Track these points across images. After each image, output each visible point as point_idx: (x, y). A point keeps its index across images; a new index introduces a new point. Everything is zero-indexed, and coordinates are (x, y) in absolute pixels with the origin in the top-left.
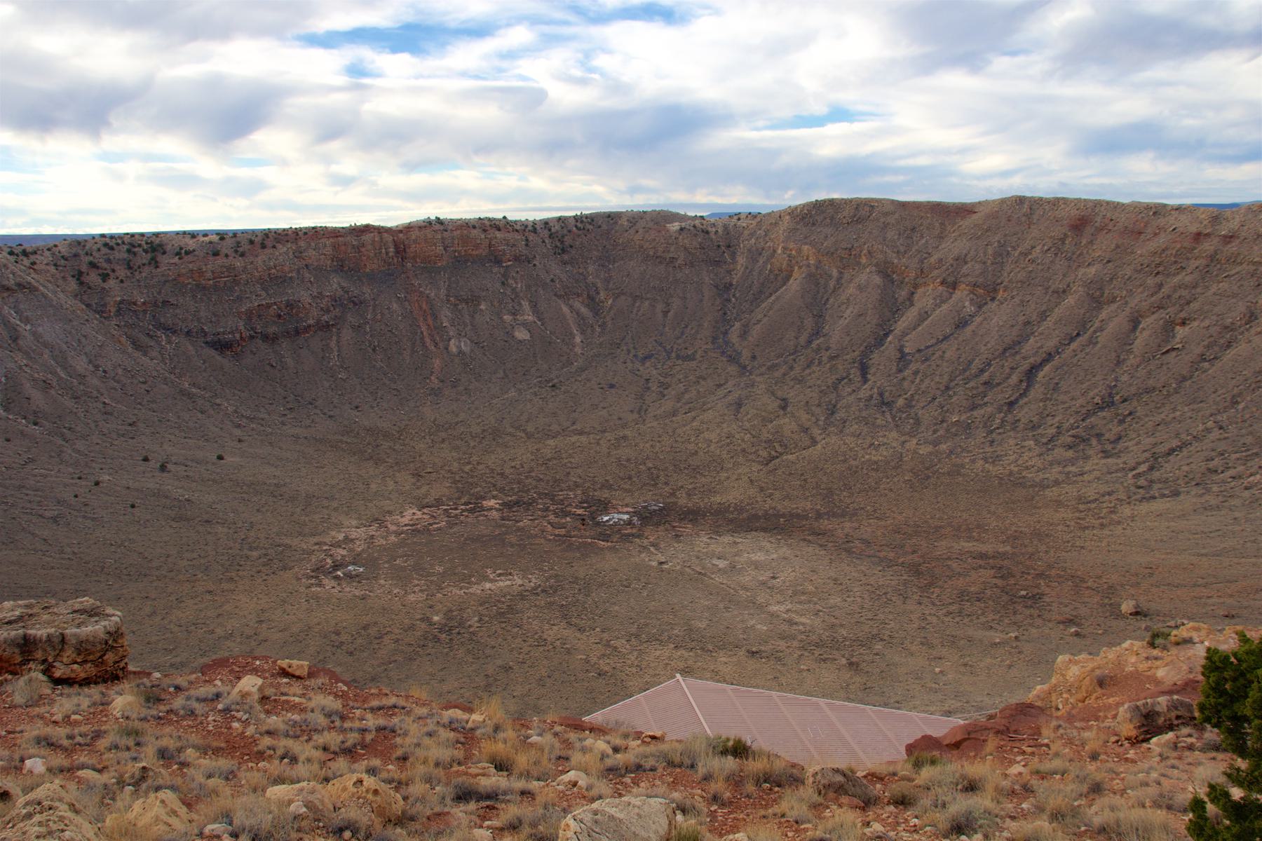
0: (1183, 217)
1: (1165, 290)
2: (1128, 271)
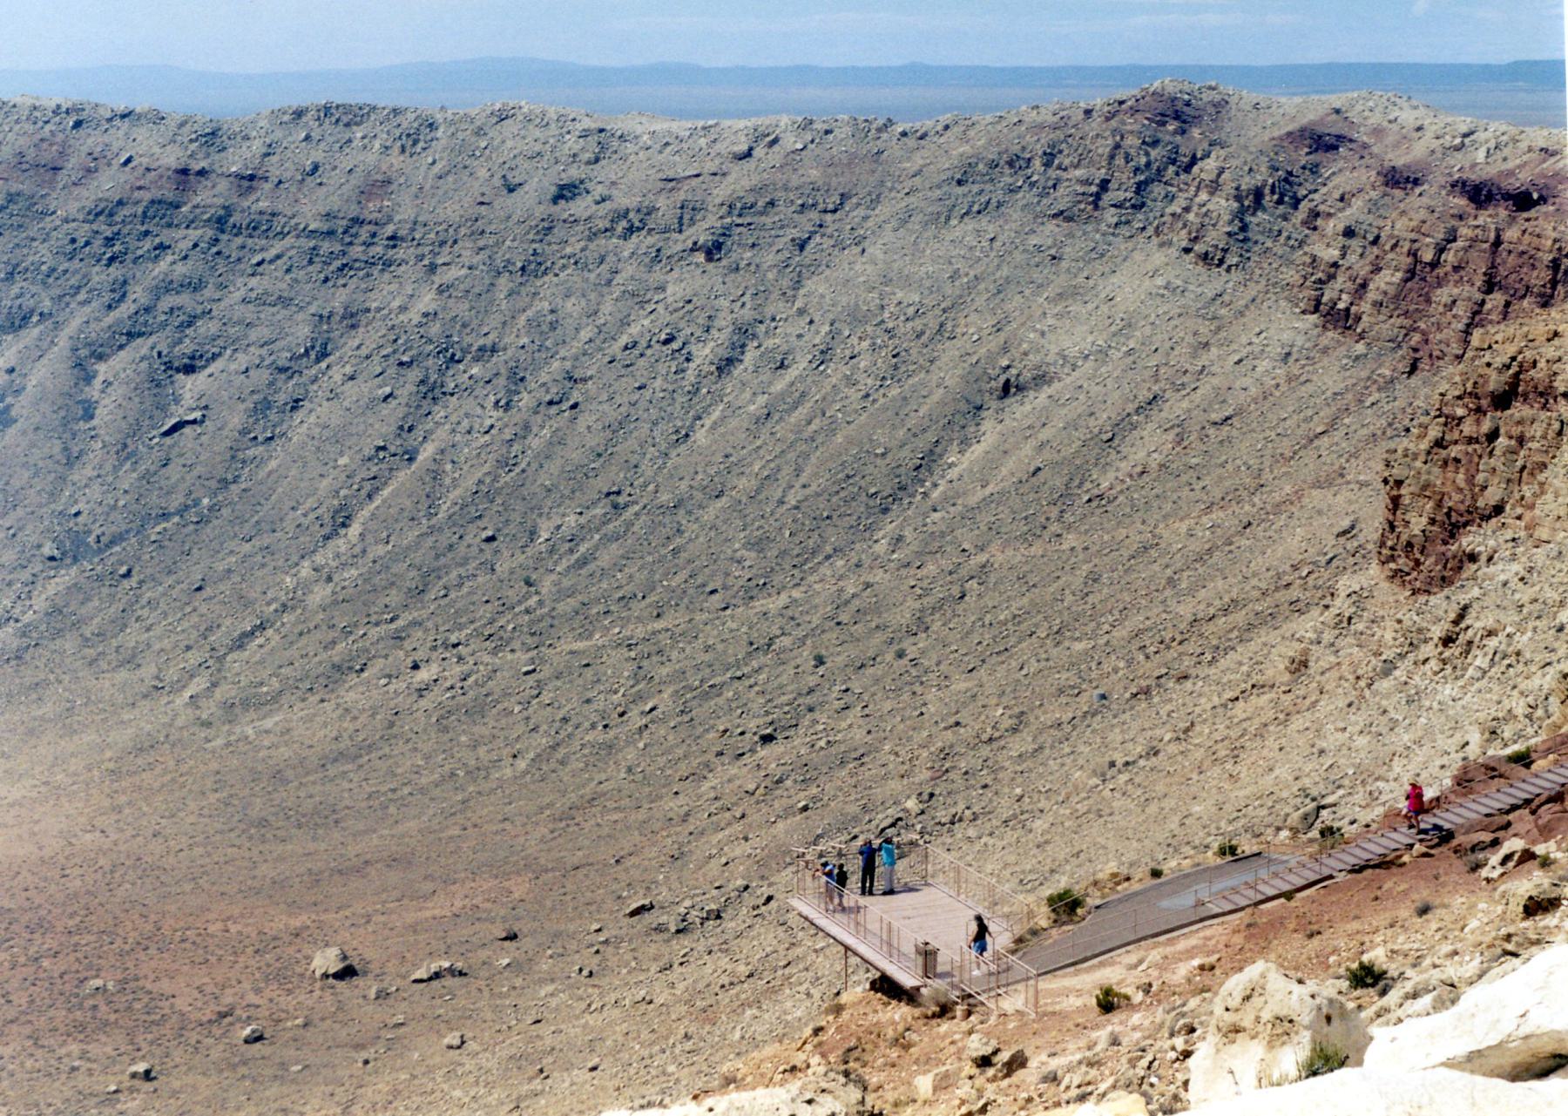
0: (141, 133)
1: (138, 294)
2: (43, 254)
